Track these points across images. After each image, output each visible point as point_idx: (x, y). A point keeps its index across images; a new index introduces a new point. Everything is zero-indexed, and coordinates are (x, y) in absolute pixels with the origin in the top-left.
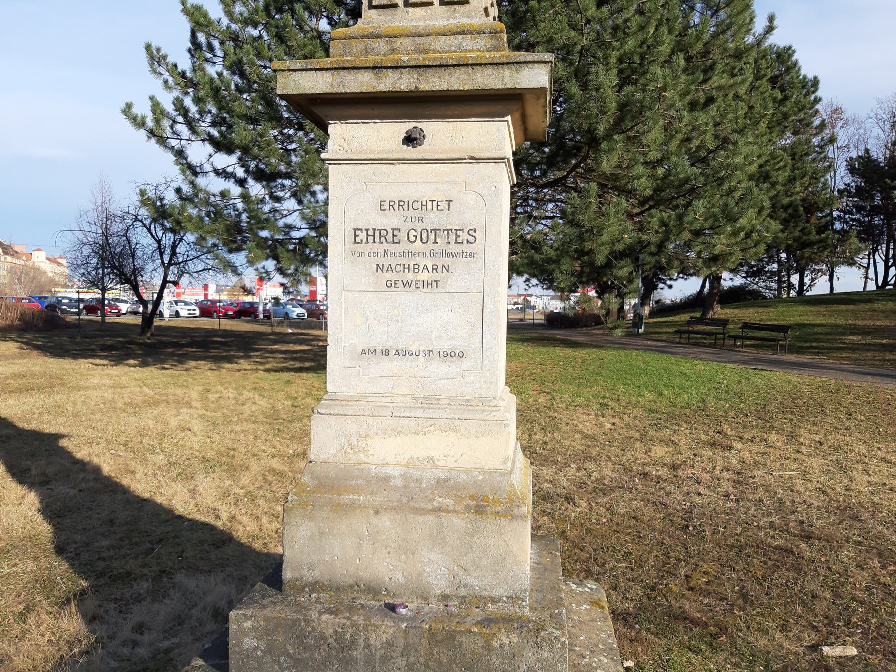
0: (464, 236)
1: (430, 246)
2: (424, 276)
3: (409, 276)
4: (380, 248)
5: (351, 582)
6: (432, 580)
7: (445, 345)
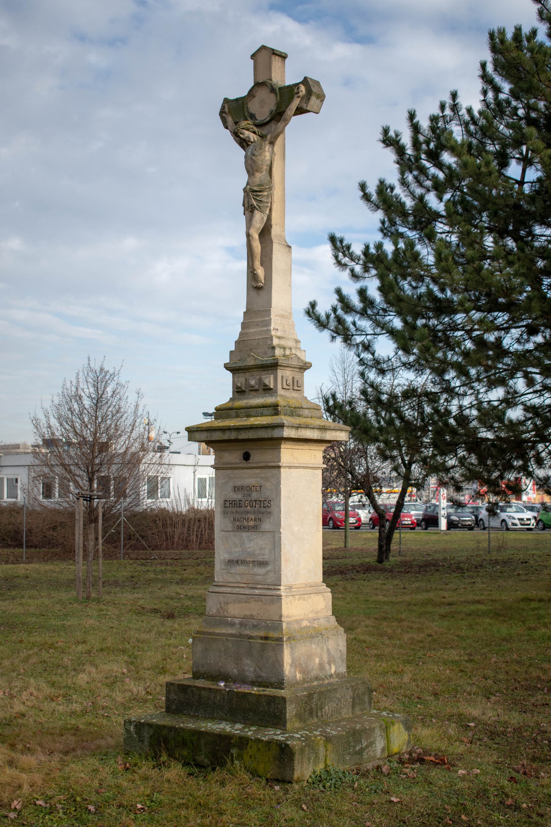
0: (266, 503)
1: (253, 509)
2: (251, 523)
3: (246, 524)
4: (234, 510)
5: (217, 673)
6: (248, 674)
7: (260, 558)
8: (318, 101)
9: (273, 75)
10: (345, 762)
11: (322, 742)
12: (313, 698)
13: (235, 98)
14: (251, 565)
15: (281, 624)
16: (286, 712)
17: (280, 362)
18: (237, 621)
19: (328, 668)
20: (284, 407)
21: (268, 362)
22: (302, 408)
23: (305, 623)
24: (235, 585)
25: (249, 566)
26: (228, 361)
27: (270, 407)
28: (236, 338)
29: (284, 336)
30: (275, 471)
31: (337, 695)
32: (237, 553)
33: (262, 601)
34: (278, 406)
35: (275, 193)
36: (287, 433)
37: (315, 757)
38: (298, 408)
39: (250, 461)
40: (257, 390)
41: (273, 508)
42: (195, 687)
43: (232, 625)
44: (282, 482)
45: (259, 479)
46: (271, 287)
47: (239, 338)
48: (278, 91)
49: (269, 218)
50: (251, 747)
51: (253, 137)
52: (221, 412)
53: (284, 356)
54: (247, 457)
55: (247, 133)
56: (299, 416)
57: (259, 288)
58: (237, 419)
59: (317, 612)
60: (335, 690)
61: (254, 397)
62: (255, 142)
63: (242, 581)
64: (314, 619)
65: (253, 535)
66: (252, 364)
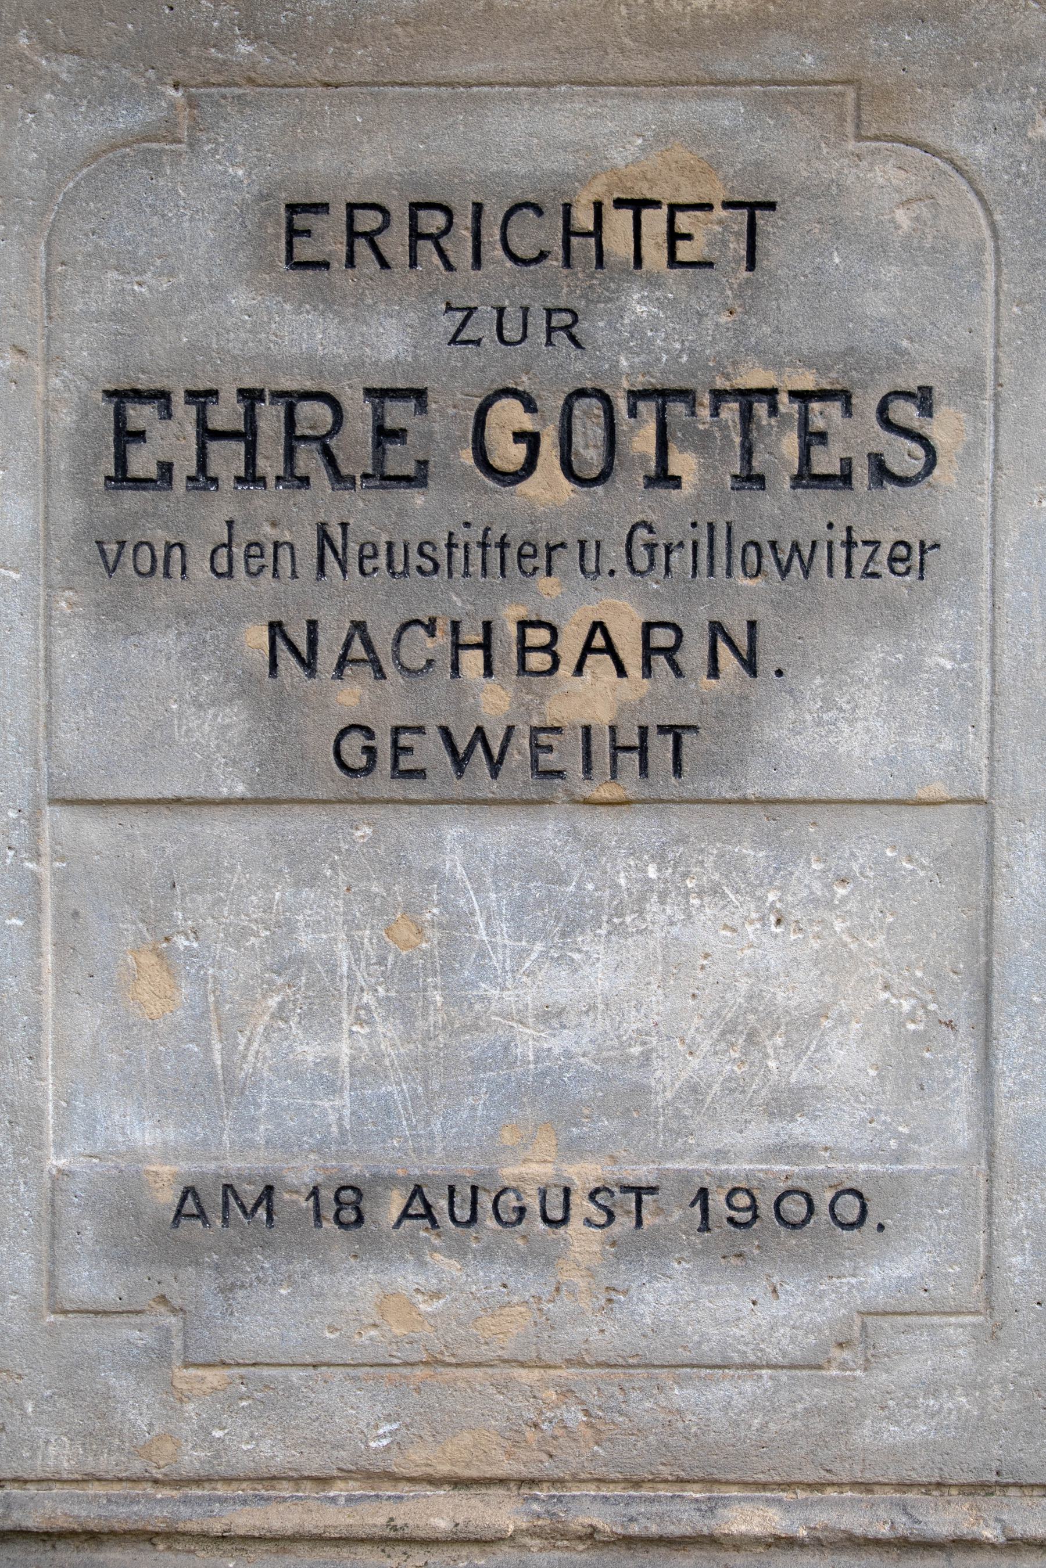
0: (853, 436)
1: (628, 500)
2: (593, 697)
3: (493, 701)
4: (287, 516)
7: (739, 1149)
14: (581, 1239)
25: (544, 1258)
32: (323, 1080)
45: (726, 111)
63: (419, 1458)
65: (618, 848)
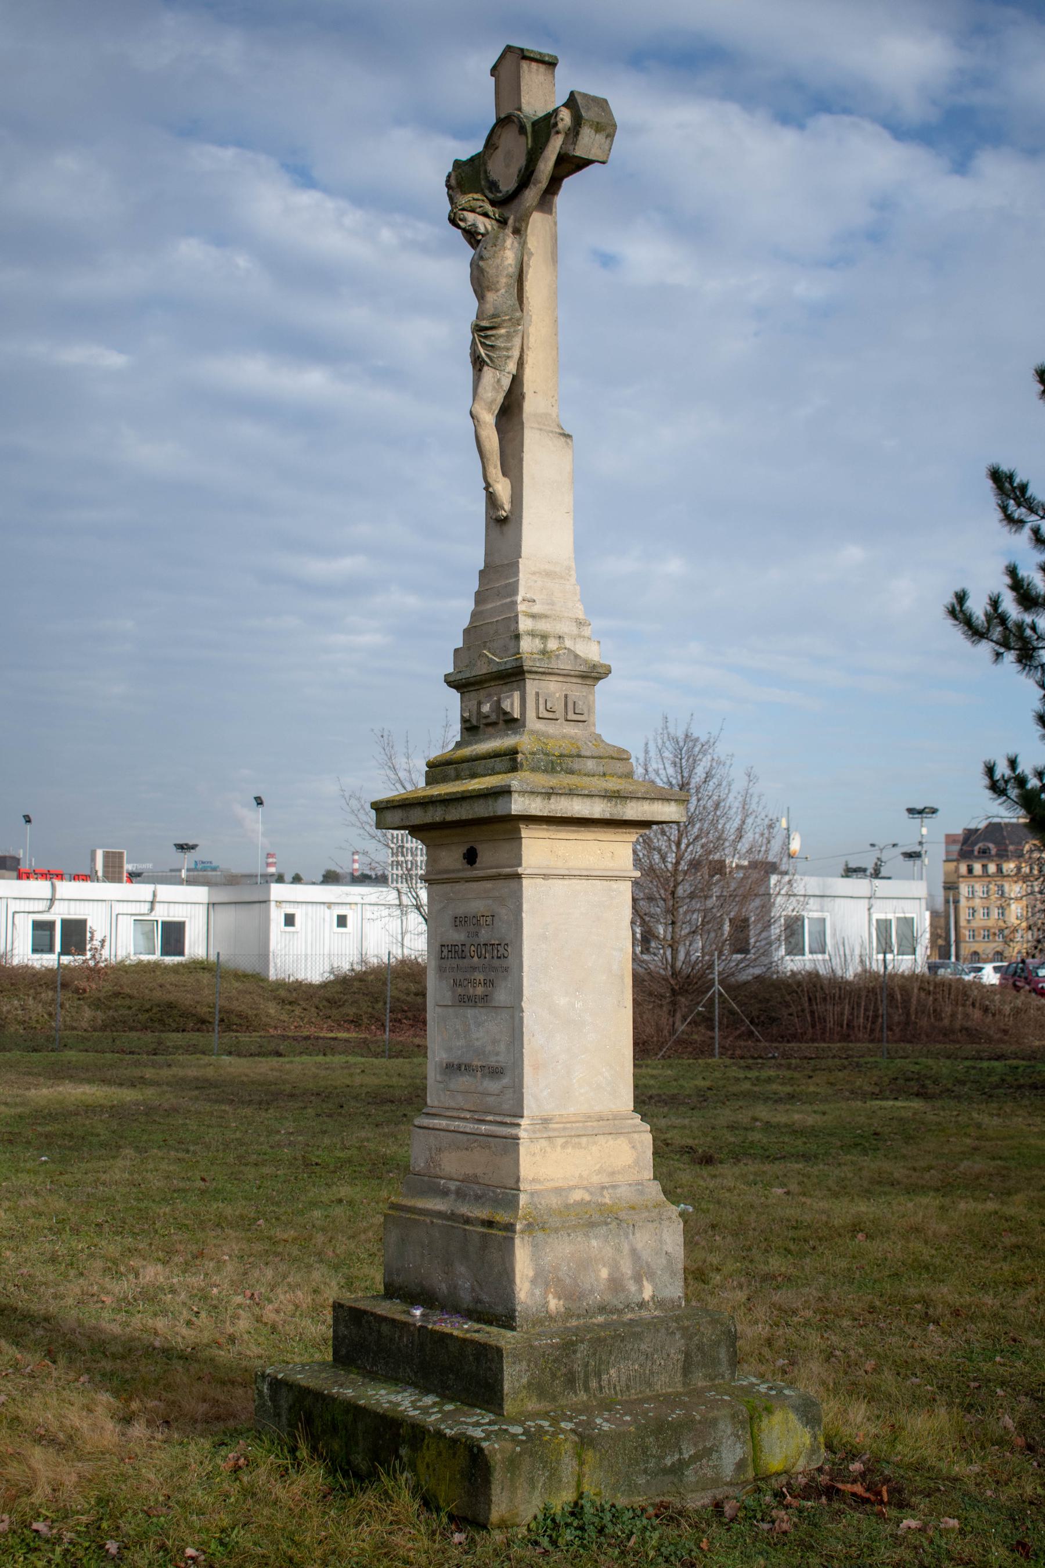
1: (482, 960)
2: (480, 990)
7: (492, 1061)
8: (600, 138)
9: (524, 101)
10: (632, 1489)
11: (568, 1446)
12: (575, 1352)
13: (469, 157)
15: (518, 1196)
16: (502, 1380)
17: (527, 665)
18: (453, 1186)
19: (633, 1288)
20: (533, 753)
21: (508, 666)
22: (579, 756)
23: (577, 1196)
24: (455, 1114)
25: (475, 1077)
26: (451, 669)
27: (505, 755)
28: (466, 623)
29: (549, 613)
30: (513, 884)
31: (643, 1347)
33: (490, 1148)
34: (517, 753)
35: (532, 330)
36: (518, 805)
37: (549, 1478)
38: (570, 756)
39: (477, 865)
40: (494, 724)
41: (511, 960)
42: (372, 1314)
43: (445, 1193)
44: (525, 907)
45: (490, 902)
46: (521, 517)
47: (471, 623)
48: (529, 129)
49: (517, 381)
50: (428, 1448)
51: (483, 225)
52: (438, 770)
53: (544, 652)
54: (471, 857)
55: (470, 217)
56: (572, 772)
57: (502, 521)
58: (457, 783)
59: (613, 1173)
60: (638, 1336)
61: (491, 737)
62: (487, 232)
63: (466, 1107)
64: (603, 1188)
66: (484, 671)
